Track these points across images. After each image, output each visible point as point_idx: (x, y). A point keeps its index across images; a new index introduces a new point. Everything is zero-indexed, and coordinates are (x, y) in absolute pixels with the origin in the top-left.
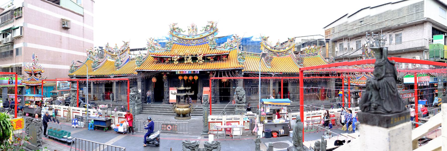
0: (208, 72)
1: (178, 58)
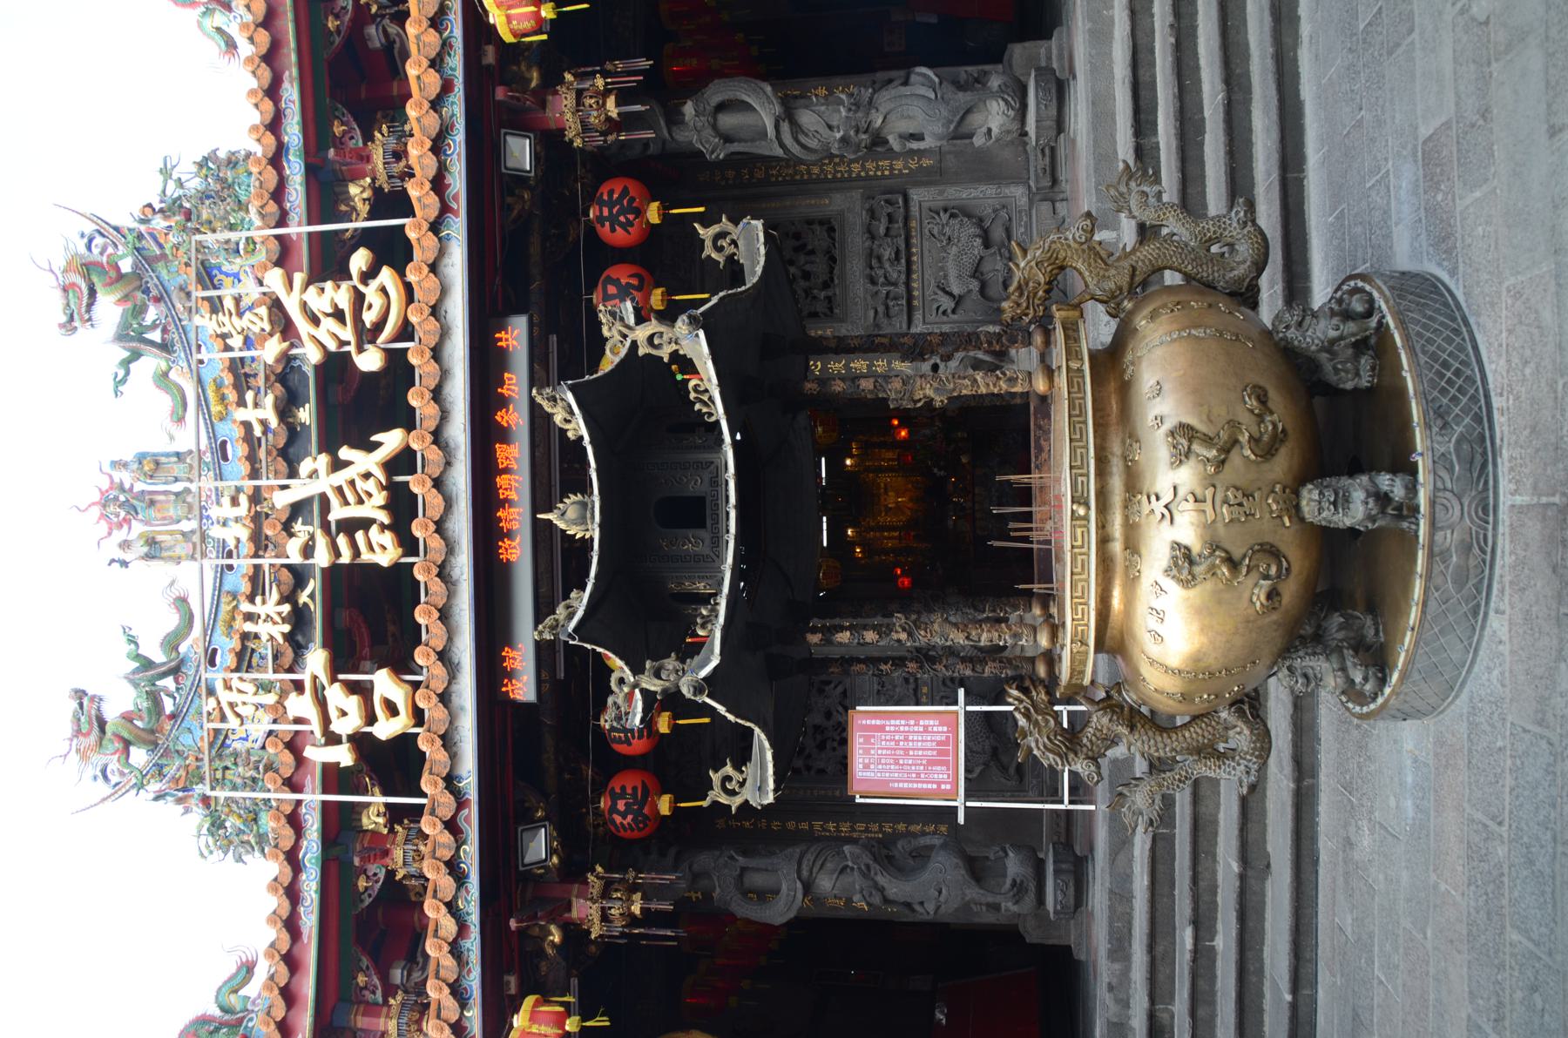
0: (520, 152)
1: (316, 660)
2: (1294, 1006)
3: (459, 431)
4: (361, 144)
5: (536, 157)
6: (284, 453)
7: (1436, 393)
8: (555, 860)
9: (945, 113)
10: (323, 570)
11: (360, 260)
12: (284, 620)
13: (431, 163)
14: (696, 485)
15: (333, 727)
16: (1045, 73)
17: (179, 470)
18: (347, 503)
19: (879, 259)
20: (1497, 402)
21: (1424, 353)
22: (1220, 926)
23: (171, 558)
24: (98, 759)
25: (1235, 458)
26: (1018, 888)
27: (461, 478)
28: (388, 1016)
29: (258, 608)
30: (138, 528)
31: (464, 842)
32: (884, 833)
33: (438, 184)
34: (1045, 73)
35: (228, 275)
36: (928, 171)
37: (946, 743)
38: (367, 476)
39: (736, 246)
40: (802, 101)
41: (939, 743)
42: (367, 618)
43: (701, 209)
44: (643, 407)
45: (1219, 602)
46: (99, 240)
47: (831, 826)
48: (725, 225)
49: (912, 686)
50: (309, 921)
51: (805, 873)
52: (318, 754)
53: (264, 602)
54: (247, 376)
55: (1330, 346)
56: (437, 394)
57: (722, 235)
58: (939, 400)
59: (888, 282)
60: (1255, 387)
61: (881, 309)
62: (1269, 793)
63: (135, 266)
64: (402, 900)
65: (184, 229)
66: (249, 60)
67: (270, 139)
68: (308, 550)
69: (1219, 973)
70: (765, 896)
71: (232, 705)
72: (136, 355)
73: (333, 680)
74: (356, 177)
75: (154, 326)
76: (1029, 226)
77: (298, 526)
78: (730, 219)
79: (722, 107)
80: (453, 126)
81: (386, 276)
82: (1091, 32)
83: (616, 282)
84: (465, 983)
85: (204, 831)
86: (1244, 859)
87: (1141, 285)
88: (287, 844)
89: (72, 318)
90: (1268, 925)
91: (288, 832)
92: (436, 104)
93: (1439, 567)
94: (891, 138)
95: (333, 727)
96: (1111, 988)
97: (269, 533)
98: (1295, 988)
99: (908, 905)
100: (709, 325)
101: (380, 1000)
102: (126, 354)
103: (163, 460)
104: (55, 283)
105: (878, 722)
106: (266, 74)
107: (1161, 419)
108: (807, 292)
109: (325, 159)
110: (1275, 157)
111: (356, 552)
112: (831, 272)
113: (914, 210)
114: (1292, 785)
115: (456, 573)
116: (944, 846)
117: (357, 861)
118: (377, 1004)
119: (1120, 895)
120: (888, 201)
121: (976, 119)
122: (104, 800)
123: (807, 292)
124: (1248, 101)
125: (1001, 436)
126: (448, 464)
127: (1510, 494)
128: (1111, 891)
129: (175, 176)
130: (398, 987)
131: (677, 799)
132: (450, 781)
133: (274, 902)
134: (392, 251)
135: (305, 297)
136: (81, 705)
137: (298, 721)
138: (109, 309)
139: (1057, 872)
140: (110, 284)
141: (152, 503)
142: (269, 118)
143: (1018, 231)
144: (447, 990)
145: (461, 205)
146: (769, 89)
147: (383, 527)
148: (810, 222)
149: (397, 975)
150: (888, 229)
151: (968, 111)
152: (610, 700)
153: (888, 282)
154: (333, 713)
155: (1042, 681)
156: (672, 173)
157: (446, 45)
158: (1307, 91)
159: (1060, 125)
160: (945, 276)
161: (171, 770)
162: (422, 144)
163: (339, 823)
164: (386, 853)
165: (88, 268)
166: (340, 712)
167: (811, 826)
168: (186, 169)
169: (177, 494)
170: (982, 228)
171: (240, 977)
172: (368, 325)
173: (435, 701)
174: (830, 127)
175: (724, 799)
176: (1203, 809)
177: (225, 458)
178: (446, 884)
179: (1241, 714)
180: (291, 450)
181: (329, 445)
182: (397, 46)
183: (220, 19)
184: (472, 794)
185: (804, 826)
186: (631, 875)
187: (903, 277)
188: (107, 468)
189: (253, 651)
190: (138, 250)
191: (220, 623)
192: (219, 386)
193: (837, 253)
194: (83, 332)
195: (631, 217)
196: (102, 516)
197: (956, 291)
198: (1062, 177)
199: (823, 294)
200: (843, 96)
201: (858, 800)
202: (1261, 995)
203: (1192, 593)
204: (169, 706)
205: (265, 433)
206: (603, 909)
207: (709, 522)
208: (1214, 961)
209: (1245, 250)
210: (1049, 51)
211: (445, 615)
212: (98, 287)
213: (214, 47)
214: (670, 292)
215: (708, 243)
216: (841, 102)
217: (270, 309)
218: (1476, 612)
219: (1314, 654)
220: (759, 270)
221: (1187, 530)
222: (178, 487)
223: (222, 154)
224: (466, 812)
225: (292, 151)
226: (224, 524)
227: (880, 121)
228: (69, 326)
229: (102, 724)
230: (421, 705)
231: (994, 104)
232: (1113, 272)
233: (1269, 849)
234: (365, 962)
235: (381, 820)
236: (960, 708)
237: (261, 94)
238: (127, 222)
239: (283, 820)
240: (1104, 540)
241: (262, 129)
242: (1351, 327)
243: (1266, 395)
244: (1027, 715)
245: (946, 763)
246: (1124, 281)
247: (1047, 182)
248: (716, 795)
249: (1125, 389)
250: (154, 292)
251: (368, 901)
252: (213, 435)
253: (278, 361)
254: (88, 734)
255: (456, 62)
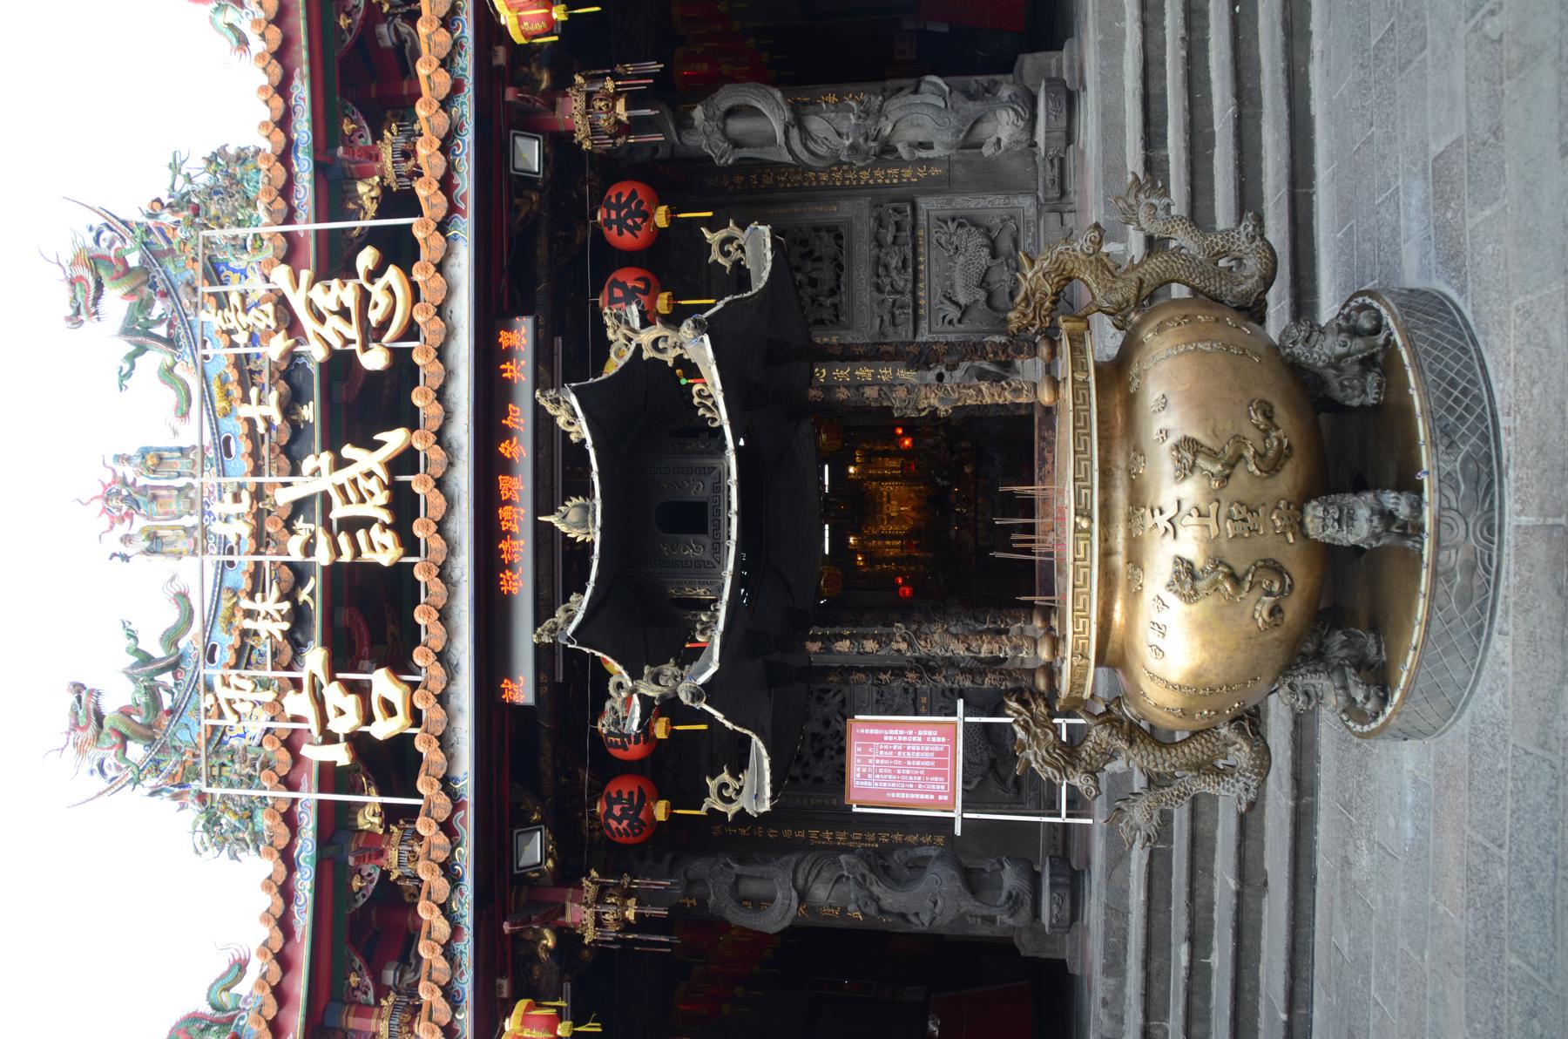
0: (529, 154)
1: (315, 658)
2: (1289, 1026)
3: (462, 432)
4: (370, 143)
5: (545, 159)
6: (287, 450)
7: (1442, 412)
8: (550, 863)
9: (955, 122)
10: (324, 568)
11: (366, 258)
12: (284, 618)
13: (440, 162)
14: (698, 491)
15: (330, 726)
16: (1055, 83)
17: (182, 465)
18: (349, 502)
19: (886, 267)
20: (1503, 422)
21: (1432, 371)
22: (1215, 944)
23: (172, 553)
24: (95, 754)
25: (1240, 473)
26: (1014, 901)
27: (463, 479)
28: (379, 1017)
29: (257, 605)
30: (140, 522)
31: (459, 844)
32: (880, 843)
33: (446, 184)
34: (1055, 83)
35: (235, 271)
36: (937, 179)
37: (943, 754)
38: (370, 475)
39: (743, 251)
40: (812, 108)
41: (937, 754)
42: (367, 617)
43: (709, 214)
44: (646, 410)
45: (1222, 618)
46: (107, 234)
47: (828, 835)
48: (732, 229)
49: (911, 696)
50: (303, 920)
51: (800, 882)
52: (315, 753)
53: (264, 599)
54: (252, 372)
55: (1337, 363)
56: (441, 395)
57: (729, 240)
58: (944, 410)
59: (895, 291)
60: (1260, 402)
61: (887, 318)
62: (1267, 810)
63: (143, 260)
64: (395, 901)
65: (192, 224)
66: (260, 57)
67: (279, 136)
68: (309, 548)
69: (1214, 990)
70: (760, 903)
71: (230, 702)
72: (141, 350)
73: (332, 679)
74: (364, 175)
75: (160, 321)
76: (1036, 236)
77: (300, 524)
78: (737, 224)
79: (731, 112)
80: (462, 126)
81: (393, 274)
82: (1103, 44)
83: (623, 286)
84: (457, 986)
85: (200, 827)
86: (1241, 876)
87: (1148, 298)
88: (282, 842)
89: (78, 312)
90: (1264, 944)
91: (284, 830)
92: (446, 104)
93: (1443, 587)
94: (900, 146)
95: (330, 726)
96: (1105, 1003)
97: (270, 529)
98: (1290, 1009)
99: (903, 916)
100: (714, 329)
101: (372, 1001)
102: (132, 348)
103: (166, 454)
104: (62, 276)
105: (877, 732)
106: (277, 70)
107: (1166, 433)
108: (814, 299)
109: (334, 157)
110: (1285, 172)
111: (357, 551)
112: (838, 277)
113: (922, 219)
114: (1291, 803)
115: (456, 574)
116: (940, 857)
117: (351, 861)
118: (368, 1005)
119: (1116, 910)
120: (896, 207)
121: (985, 129)
122: (100, 794)
123: (814, 299)
124: (1258, 116)
125: (1003, 449)
126: (451, 464)
127: (1516, 515)
128: (1107, 906)
129: (184, 171)
130: (390, 988)
131: (673, 806)
132: (447, 782)
133: (268, 901)
134: (399, 250)
135: (312, 294)
136: (79, 699)
137: (295, 719)
138: (116, 303)
139: (1053, 886)
140: (117, 278)
141: (155, 498)
142: (278, 115)
143: (1026, 242)
144: (439, 993)
145: (469, 206)
146: (778, 95)
147: (385, 527)
148: (817, 229)
149: (389, 976)
150: (895, 237)
151: (978, 121)
152: (608, 705)
153: (895, 291)
154: (331, 712)
155: (1041, 694)
156: (679, 178)
157: (457, 45)
158: (1318, 107)
159: (1069, 137)
160: (952, 286)
161: (167, 766)
162: (431, 143)
163: (334, 822)
164: (381, 853)
165: (95, 262)
166: (338, 711)
167: (807, 835)
168: (195, 164)
169: (180, 490)
170: (989, 238)
171: (232, 976)
172: (374, 324)
173: (433, 703)
174: (840, 135)
175: (720, 807)
176: (1201, 826)
177: (229, 454)
178: (440, 886)
179: (1241, 730)
180: (294, 448)
181: (332, 443)
182: (408, 45)
183: (232, 15)
184: (469, 796)
185: (801, 834)
186: (626, 880)
187: (910, 285)
188: (110, 462)
189: (252, 648)
190: (145, 244)
191: (219, 620)
192: (223, 382)
193: (844, 261)
194: (89, 325)
195: (639, 220)
196: (105, 510)
197: (962, 301)
198: (1071, 188)
199: (829, 302)
200: (853, 104)
201: (855, 809)
202: (1256, 1014)
203: (1194, 608)
204: (167, 702)
205: (268, 430)
206: (597, 914)
207: (710, 528)
208: (1210, 979)
209: (1253, 265)
210: (1060, 61)
211: (444, 616)
212: (105, 281)
213: (227, 42)
214: (676, 297)
215: (715, 248)
216: (850, 109)
217: (275, 306)
218: (1480, 632)
219: (1316, 671)
220: (765, 275)
221: (1190, 544)
222: (181, 482)
223: (231, 150)
224: (461, 814)
225: (301, 148)
226: (226, 521)
227: (889, 129)
228: (75, 319)
229: (100, 718)
230: (419, 706)
231: (1004, 114)
232: (1120, 284)
233: (1267, 866)
234: (358, 962)
235: (377, 820)
236: (959, 719)
237: (271, 91)
238: (135, 216)
239: (279, 819)
240: (1107, 554)
241: (272, 125)
242: (1358, 343)
243: (1271, 410)
244: (1026, 728)
245: (943, 774)
246: (1131, 293)
247: (1055, 194)
248: (713, 802)
249: (1131, 402)
250: (161, 287)
251: (361, 901)
252: (216, 431)
253: (283, 358)
254: (85, 728)
255: (466, 63)
